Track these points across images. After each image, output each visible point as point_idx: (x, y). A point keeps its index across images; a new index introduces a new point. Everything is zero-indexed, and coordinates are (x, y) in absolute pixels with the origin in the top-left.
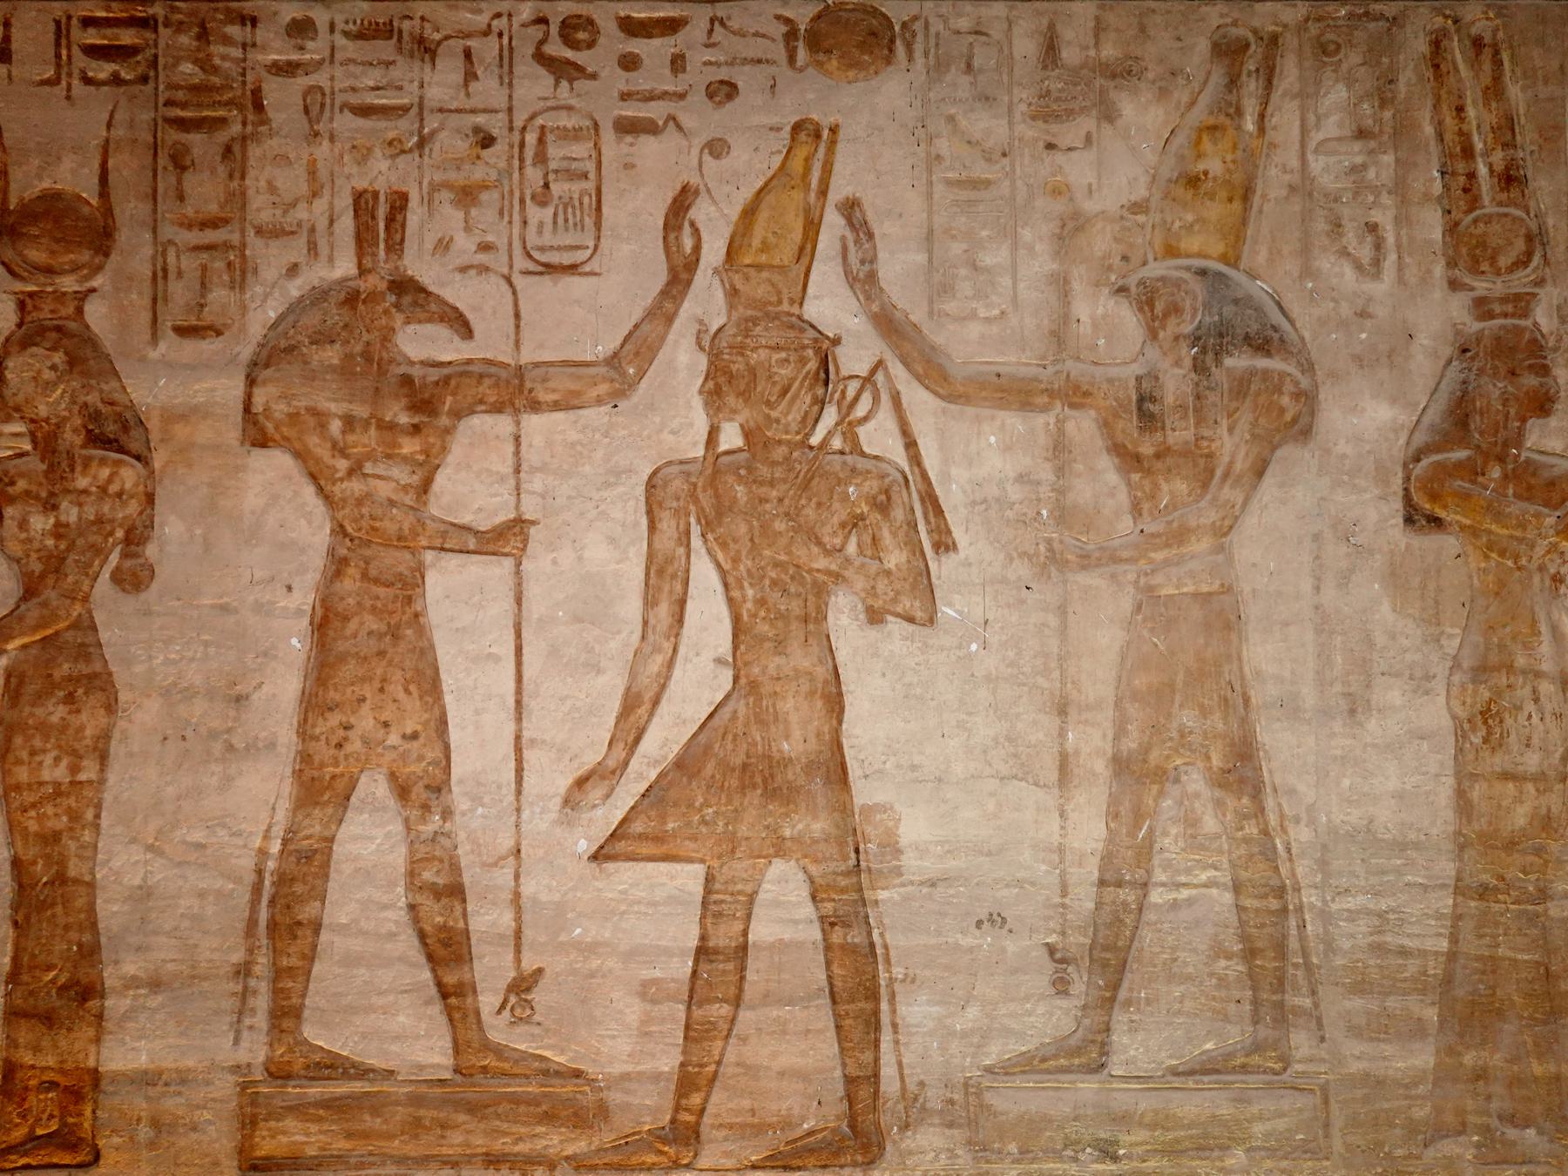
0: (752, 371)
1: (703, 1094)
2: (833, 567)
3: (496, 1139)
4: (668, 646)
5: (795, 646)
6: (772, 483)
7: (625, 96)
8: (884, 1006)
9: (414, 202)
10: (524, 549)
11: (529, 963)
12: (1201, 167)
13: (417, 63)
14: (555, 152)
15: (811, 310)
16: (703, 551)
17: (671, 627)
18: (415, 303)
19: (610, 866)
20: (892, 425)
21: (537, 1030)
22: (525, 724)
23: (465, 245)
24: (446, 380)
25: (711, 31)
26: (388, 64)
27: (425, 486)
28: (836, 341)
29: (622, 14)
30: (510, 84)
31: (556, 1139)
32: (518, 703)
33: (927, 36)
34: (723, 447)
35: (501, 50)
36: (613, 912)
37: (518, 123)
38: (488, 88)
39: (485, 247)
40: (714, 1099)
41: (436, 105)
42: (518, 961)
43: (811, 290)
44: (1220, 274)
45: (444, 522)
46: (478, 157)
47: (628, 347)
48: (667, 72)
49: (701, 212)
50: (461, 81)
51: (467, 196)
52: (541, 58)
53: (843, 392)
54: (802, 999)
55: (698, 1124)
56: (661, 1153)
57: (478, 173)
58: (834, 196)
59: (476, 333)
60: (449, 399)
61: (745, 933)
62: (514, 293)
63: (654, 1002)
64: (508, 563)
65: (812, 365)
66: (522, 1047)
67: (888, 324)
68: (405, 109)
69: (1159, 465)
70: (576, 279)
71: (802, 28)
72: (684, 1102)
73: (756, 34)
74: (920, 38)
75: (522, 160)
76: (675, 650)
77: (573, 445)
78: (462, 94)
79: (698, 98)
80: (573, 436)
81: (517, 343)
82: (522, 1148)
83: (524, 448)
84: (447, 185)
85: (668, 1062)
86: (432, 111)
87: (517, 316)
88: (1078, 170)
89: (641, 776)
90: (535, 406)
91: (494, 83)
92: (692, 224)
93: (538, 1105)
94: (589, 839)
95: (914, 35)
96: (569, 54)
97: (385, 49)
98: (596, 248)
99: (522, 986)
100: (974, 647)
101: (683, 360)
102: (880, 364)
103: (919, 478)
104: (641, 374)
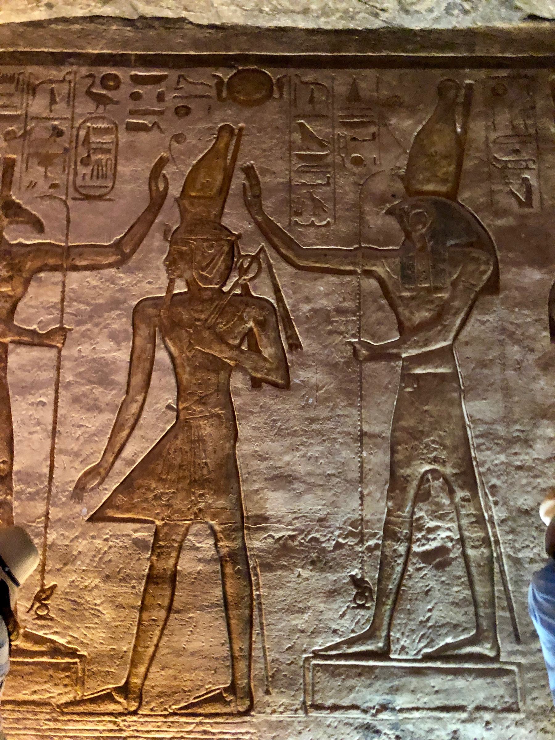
0: (191, 250)
1: (146, 665)
2: (234, 356)
3: (19, 691)
4: (140, 398)
5: (213, 400)
6: (202, 311)
7: (133, 113)
8: (256, 612)
9: (18, 163)
10: (63, 344)
11: (49, 582)
12: (433, 150)
13: (25, 97)
14: (94, 139)
15: (225, 222)
16: (162, 346)
17: (142, 388)
18: (16, 215)
19: (101, 524)
20: (268, 282)
21: (50, 623)
22: (56, 441)
23: (43, 186)
24: (29, 253)
25: (178, 82)
26: (11, 95)
27: (13, 310)
28: (239, 237)
29: (133, 73)
30: (74, 106)
31: (56, 691)
32: (54, 428)
33: (290, 86)
34: (175, 292)
35: (70, 89)
36: (99, 551)
37: (77, 125)
38: (61, 108)
39: (53, 186)
40: (153, 669)
41: (34, 115)
42: (43, 578)
43: (226, 210)
44: (445, 204)
45: (20, 328)
46: (55, 141)
47: (127, 237)
48: (155, 101)
49: (168, 170)
50: (48, 103)
51: (46, 161)
52: (89, 93)
53: (242, 263)
54: (208, 607)
55: (143, 684)
56: (119, 703)
57: (54, 150)
58: (239, 163)
59: (47, 229)
60: (29, 264)
61: (176, 565)
62: (68, 209)
63: (120, 606)
64: (54, 352)
65: (226, 249)
66: (40, 633)
67: (267, 230)
68: (18, 116)
69: (413, 303)
70: (101, 203)
71: (226, 80)
72: (134, 671)
73: (202, 83)
74: (285, 90)
75: (77, 143)
76: (144, 401)
77: (95, 287)
78: (48, 111)
79: (170, 114)
80: (94, 283)
81: (67, 235)
82: (35, 697)
83: (67, 289)
84: (36, 154)
85: (127, 646)
86: (32, 119)
87: (68, 221)
88: (369, 153)
89: (120, 473)
90: (75, 268)
91: (64, 105)
92: (164, 176)
93: (47, 669)
94: (89, 509)
95: (283, 84)
96: (104, 92)
97: (10, 88)
98: (113, 188)
99: (43, 597)
100: (311, 401)
101: (156, 245)
102: (262, 249)
103: (281, 309)
104: (133, 251)
